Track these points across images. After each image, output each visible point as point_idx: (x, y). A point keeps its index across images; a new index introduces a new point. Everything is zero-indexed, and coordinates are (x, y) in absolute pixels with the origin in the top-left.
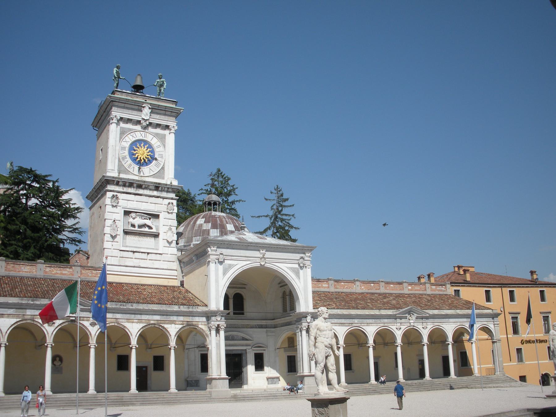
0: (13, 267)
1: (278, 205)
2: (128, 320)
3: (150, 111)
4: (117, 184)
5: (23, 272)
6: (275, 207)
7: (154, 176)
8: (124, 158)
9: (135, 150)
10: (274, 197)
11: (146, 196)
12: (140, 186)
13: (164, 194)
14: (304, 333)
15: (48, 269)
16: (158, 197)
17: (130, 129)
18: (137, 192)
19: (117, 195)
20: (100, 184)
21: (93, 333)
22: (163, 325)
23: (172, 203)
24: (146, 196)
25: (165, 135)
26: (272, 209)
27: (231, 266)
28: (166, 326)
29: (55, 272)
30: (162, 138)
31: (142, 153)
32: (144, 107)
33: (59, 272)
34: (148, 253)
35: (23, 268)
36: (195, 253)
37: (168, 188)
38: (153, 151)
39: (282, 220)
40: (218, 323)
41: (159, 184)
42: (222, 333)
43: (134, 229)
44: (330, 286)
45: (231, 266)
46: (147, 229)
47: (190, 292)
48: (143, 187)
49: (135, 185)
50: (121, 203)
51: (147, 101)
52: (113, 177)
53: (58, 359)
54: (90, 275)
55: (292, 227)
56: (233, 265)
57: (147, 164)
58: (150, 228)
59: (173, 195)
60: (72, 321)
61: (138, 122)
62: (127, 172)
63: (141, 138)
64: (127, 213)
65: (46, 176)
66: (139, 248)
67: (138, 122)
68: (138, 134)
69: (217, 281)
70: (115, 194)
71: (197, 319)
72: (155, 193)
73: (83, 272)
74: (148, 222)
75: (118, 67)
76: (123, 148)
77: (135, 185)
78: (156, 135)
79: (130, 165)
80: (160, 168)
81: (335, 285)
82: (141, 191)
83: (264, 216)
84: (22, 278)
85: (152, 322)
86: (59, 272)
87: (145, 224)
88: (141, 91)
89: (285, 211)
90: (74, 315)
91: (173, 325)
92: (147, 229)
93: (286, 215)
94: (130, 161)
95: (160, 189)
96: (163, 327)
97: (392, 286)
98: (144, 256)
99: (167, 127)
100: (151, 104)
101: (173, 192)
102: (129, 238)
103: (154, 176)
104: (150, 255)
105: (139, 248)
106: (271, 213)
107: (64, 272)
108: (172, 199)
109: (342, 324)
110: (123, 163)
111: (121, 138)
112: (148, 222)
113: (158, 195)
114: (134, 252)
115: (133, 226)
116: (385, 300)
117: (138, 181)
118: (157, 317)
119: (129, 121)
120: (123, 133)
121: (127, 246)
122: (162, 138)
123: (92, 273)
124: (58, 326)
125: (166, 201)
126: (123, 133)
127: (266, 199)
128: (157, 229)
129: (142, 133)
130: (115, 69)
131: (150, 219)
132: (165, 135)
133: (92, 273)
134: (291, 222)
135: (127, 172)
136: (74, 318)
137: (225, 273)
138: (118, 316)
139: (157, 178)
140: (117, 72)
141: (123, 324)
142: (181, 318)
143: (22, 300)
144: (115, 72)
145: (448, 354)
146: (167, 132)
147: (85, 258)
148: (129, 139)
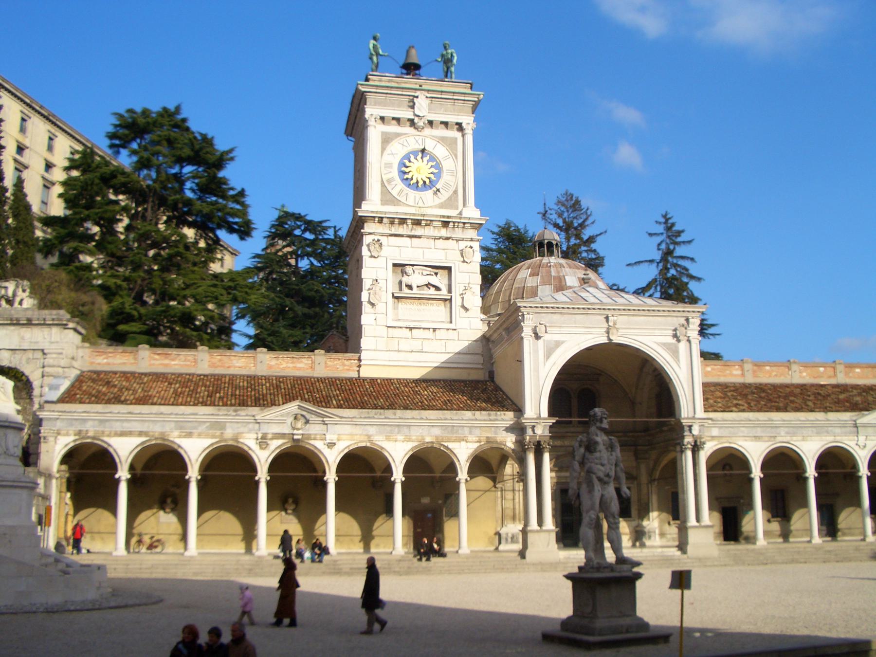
0: (220, 360)
1: (668, 241)
2: (388, 439)
3: (428, 101)
4: (381, 220)
5: (235, 367)
6: (663, 246)
7: (442, 206)
8: (389, 181)
9: (407, 167)
10: (661, 229)
11: (428, 237)
12: (417, 223)
13: (458, 233)
14: (689, 454)
15: (273, 362)
16: (448, 239)
17: (398, 135)
18: (413, 233)
19: (379, 240)
20: (354, 224)
22: (446, 444)
23: (471, 247)
24: (428, 237)
25: (456, 139)
26: (659, 249)
27: (558, 344)
28: (451, 445)
29: (284, 365)
30: (450, 143)
31: (420, 170)
32: (417, 97)
33: (291, 365)
34: (434, 330)
35: (234, 362)
36: (505, 326)
37: (464, 223)
38: (438, 166)
39: (675, 266)
41: (448, 217)
42: (546, 457)
43: (410, 291)
44: (746, 373)
45: (558, 344)
46: (432, 290)
47: (501, 390)
48: (423, 223)
49: (409, 222)
50: (385, 251)
51: (424, 87)
52: (372, 212)
53: (290, 500)
54: (341, 368)
55: (692, 277)
56: (563, 342)
57: (409, 186)
58: (437, 289)
59: (472, 233)
60: (298, 440)
62: (395, 201)
65: (321, 222)
66: (419, 321)
68: (411, 140)
69: (537, 370)
72: (444, 232)
73: (329, 363)
75: (375, 38)
76: (389, 165)
77: (409, 222)
78: (442, 140)
79: (401, 191)
80: (451, 192)
81: (754, 372)
82: (418, 231)
83: (646, 261)
84: (233, 377)
86: (291, 365)
87: (429, 284)
88: (417, 72)
89: (679, 251)
90: (300, 432)
91: (463, 443)
93: (682, 258)
94: (401, 185)
95: (451, 225)
96: (447, 448)
97: (858, 370)
98: (429, 334)
102: (402, 306)
103: (442, 206)
104: (437, 331)
105: (419, 321)
106: (657, 256)
107: (299, 365)
108: (472, 240)
109: (757, 438)
110: (389, 188)
111: (383, 149)
112: (434, 280)
113: (449, 236)
114: (411, 329)
115: (410, 287)
116: (842, 397)
117: (414, 215)
120: (386, 139)
121: (399, 320)
123: (344, 365)
124: (276, 449)
125: (462, 245)
126: (386, 139)
127: (651, 235)
128: (450, 291)
129: (417, 138)
130: (372, 42)
131: (436, 274)
132: (456, 139)
134: (693, 272)
135: (395, 201)
136: (299, 437)
137: (548, 354)
138: (372, 430)
139: (446, 208)
140: (375, 47)
141: (379, 443)
142: (477, 432)
143: (219, 410)
144: (371, 46)
145: (710, 514)
147: (341, 341)
148: (397, 150)
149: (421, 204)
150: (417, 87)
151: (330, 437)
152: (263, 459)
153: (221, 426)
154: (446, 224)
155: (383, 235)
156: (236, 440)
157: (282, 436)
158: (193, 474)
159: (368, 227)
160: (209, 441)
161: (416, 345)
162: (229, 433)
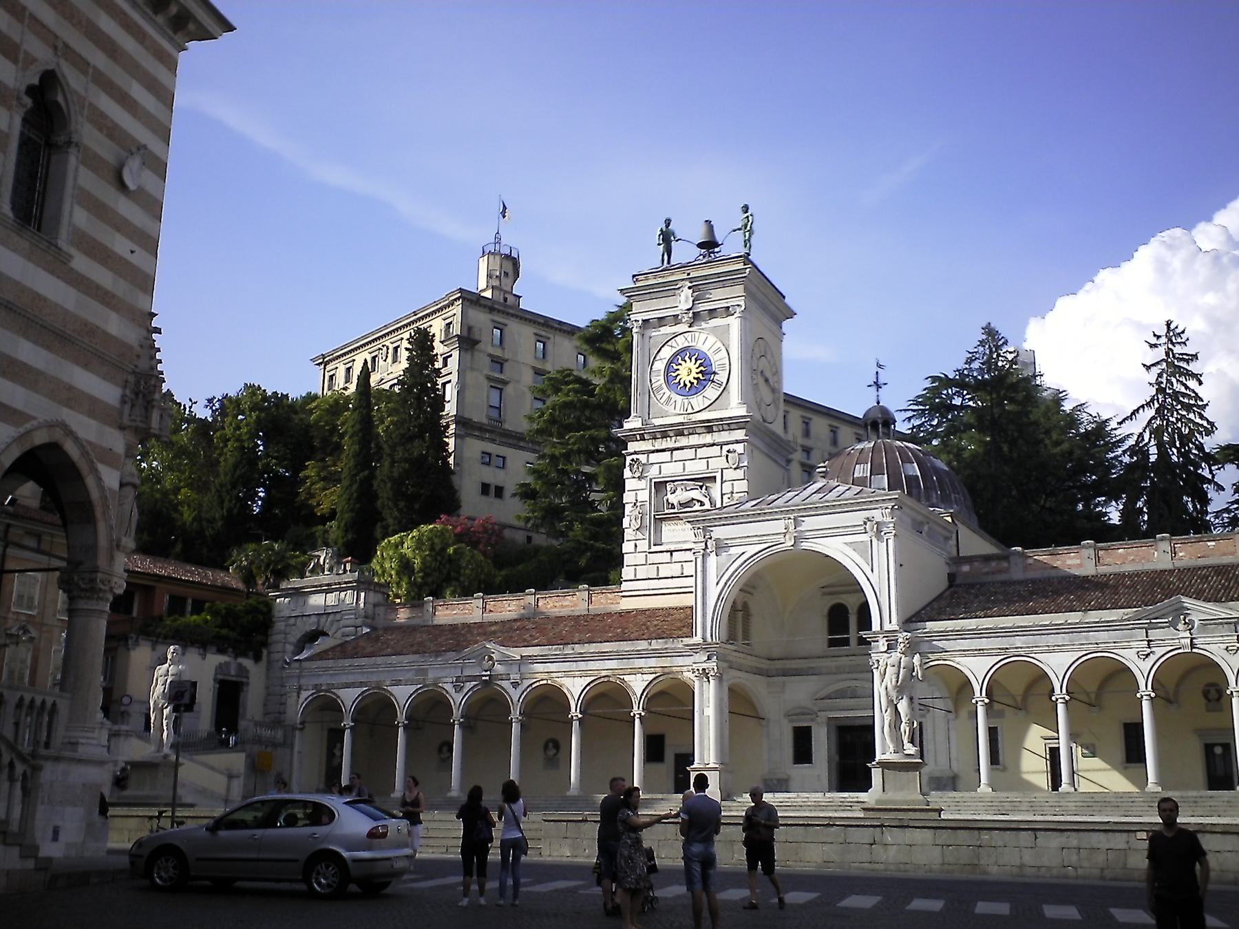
12: (680, 433)
18: (678, 445)
21: (515, 699)
24: (691, 447)
28: (626, 678)
30: (722, 334)
31: (687, 371)
40: (705, 666)
41: (709, 421)
46: (697, 507)
53: (551, 745)
59: (740, 434)
61: (676, 319)
63: (686, 344)
64: (660, 486)
67: (676, 319)
70: (635, 457)
71: (680, 661)
72: (708, 439)
74: (696, 494)
82: (683, 441)
85: (604, 673)
92: (697, 507)
99: (727, 311)
100: (691, 280)
101: (740, 427)
108: (737, 442)
109: (980, 652)
112: (696, 494)
118: (613, 664)
119: (661, 321)
122: (722, 334)
123: (607, 598)
125: (725, 448)
133: (607, 598)
142: (653, 662)
146: (730, 320)
149: (690, 411)
150: (685, 276)
151: (515, 677)
152: (457, 700)
153: (424, 672)
154: (710, 430)
155: (642, 452)
156: (436, 685)
157: (474, 678)
158: (401, 717)
159: (632, 446)
160: (414, 688)
161: (675, 569)
162: (431, 675)
